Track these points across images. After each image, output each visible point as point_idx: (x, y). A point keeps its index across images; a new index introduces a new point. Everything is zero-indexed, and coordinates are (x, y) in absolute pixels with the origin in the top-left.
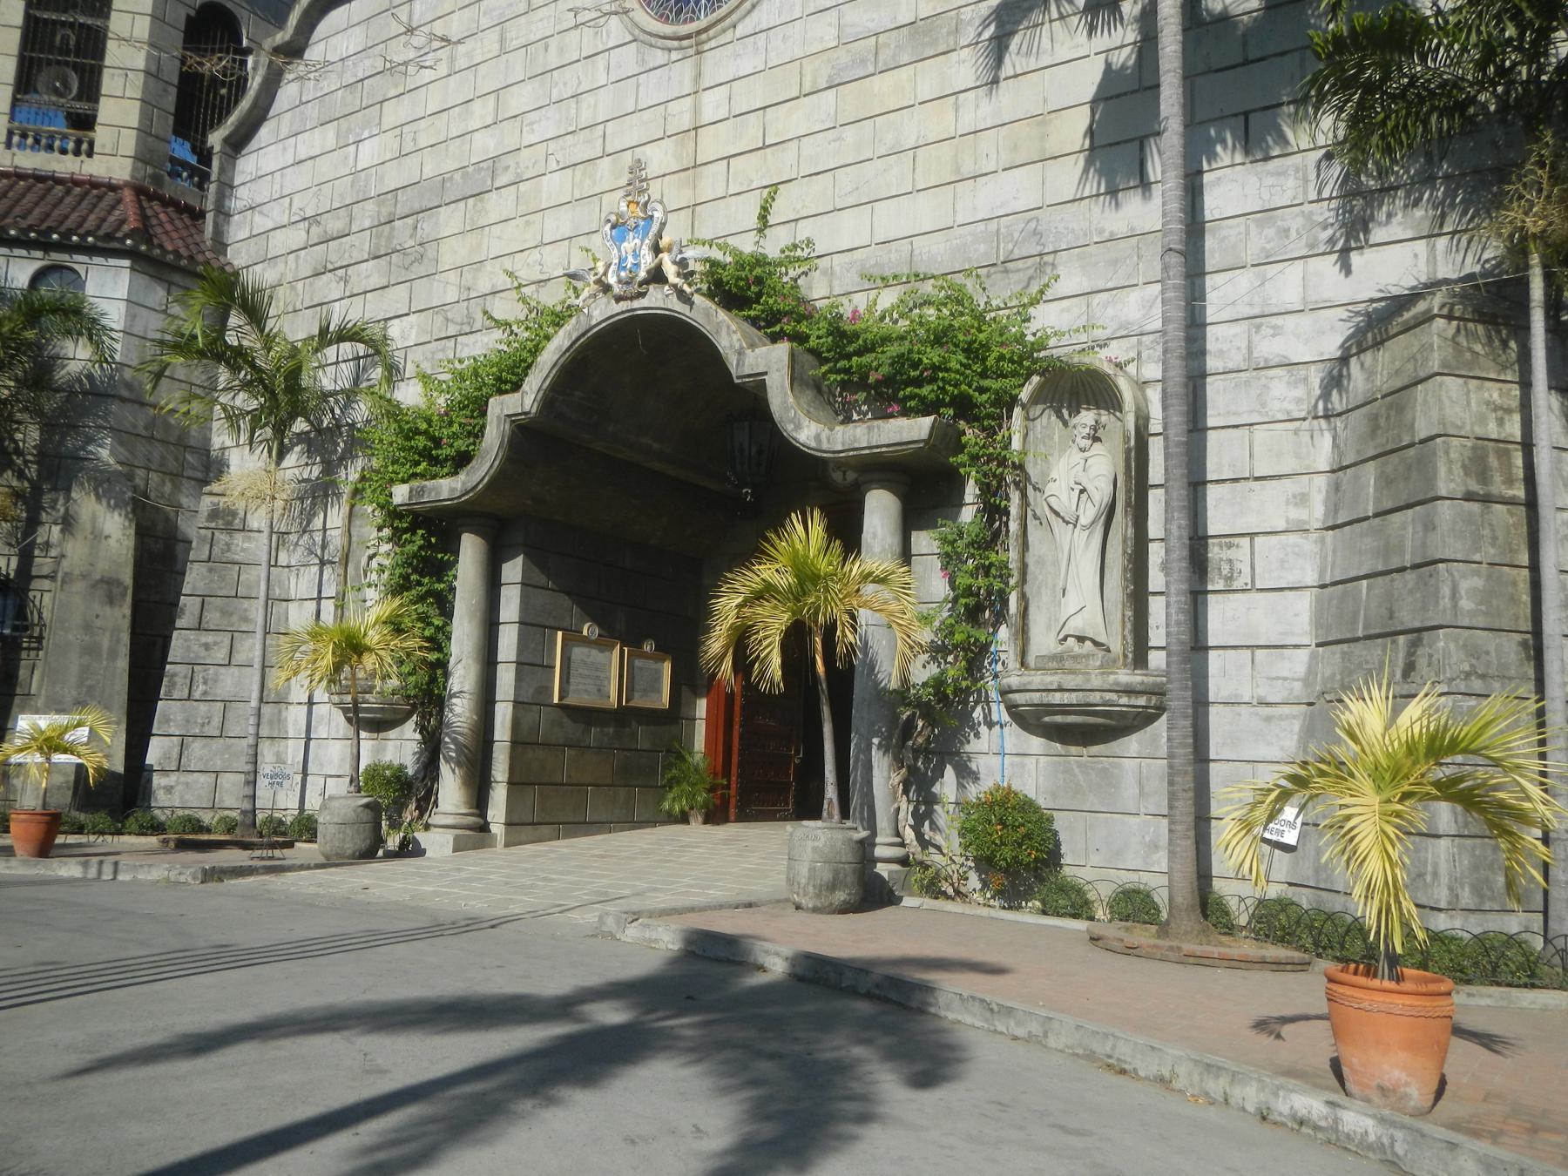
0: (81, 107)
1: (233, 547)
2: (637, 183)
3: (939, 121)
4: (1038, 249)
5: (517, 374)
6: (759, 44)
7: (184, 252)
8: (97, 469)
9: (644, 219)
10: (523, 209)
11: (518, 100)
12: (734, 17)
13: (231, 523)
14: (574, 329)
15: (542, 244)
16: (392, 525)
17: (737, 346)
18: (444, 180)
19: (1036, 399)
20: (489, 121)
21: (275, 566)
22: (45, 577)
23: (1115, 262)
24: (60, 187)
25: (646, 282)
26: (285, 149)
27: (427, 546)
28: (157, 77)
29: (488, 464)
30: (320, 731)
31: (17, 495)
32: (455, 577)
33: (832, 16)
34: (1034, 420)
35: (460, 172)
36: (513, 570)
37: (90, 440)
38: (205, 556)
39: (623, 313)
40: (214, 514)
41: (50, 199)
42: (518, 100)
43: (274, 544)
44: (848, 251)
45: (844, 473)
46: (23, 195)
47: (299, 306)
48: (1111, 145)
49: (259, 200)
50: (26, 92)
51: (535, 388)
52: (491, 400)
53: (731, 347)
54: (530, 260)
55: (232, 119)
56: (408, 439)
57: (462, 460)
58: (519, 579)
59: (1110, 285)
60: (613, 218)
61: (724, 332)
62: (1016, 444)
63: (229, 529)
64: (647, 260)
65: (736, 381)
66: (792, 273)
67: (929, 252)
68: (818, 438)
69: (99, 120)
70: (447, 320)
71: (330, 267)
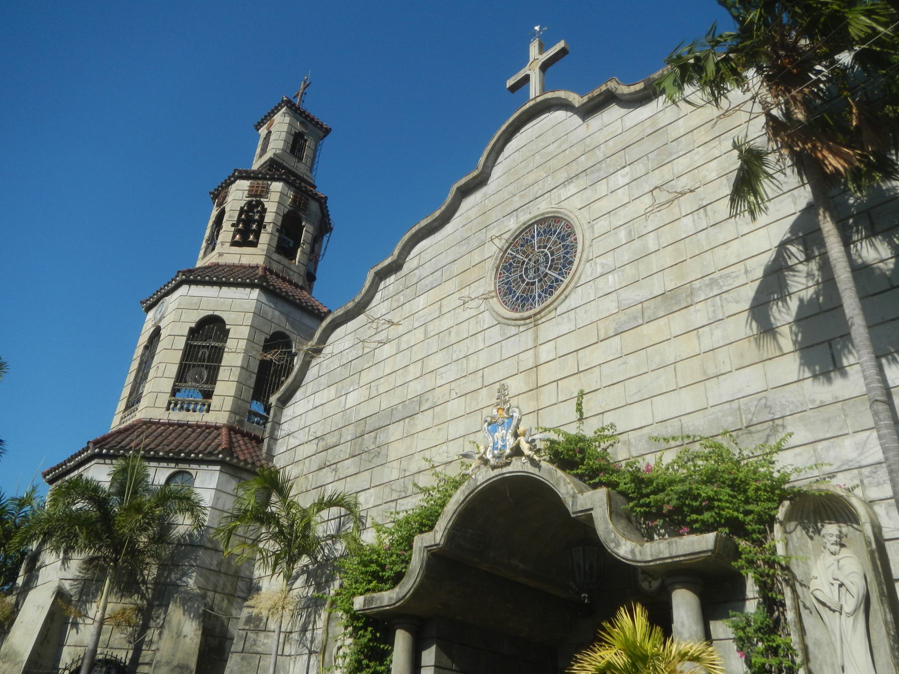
0: (206, 387)
1: (258, 642)
2: (503, 398)
3: (689, 346)
4: (770, 417)
5: (432, 521)
6: (571, 316)
7: (250, 461)
8: (186, 592)
9: (507, 418)
10: (436, 422)
11: (434, 362)
12: (555, 304)
13: (258, 626)
14: (467, 489)
15: (448, 441)
16: (352, 625)
17: (571, 492)
18: (392, 409)
19: (789, 517)
20: (418, 375)
21: (282, 655)
22: (146, 664)
23: (828, 420)
24: (190, 429)
25: (510, 456)
26: (308, 401)
27: (373, 639)
28: (247, 370)
29: (413, 581)
31: (139, 610)
32: (391, 661)
33: (613, 296)
34: (790, 533)
35: (401, 405)
36: (429, 656)
37: (185, 574)
38: (240, 649)
39: (496, 476)
40: (249, 620)
41: (184, 435)
42: (434, 362)
43: (281, 640)
44: (639, 429)
45: (650, 582)
46: (171, 434)
47: (309, 488)
48: (808, 347)
49: (293, 430)
50: (180, 382)
51: (443, 528)
52: (416, 537)
53: (568, 493)
54: (441, 451)
55: (283, 388)
56: (365, 566)
57: (398, 578)
58: (433, 663)
59: (828, 436)
60: (489, 419)
61: (562, 484)
62: (780, 551)
63: (257, 630)
64: (511, 442)
65: (573, 516)
66: (603, 446)
67: (693, 425)
68: (632, 552)
69: (214, 393)
70: (392, 490)
71: (328, 464)
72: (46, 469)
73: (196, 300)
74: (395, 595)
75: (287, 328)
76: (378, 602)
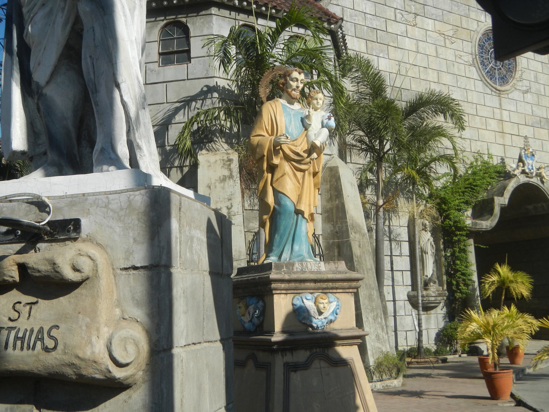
30: (401, 312)
74: (489, 225)
76: (480, 226)
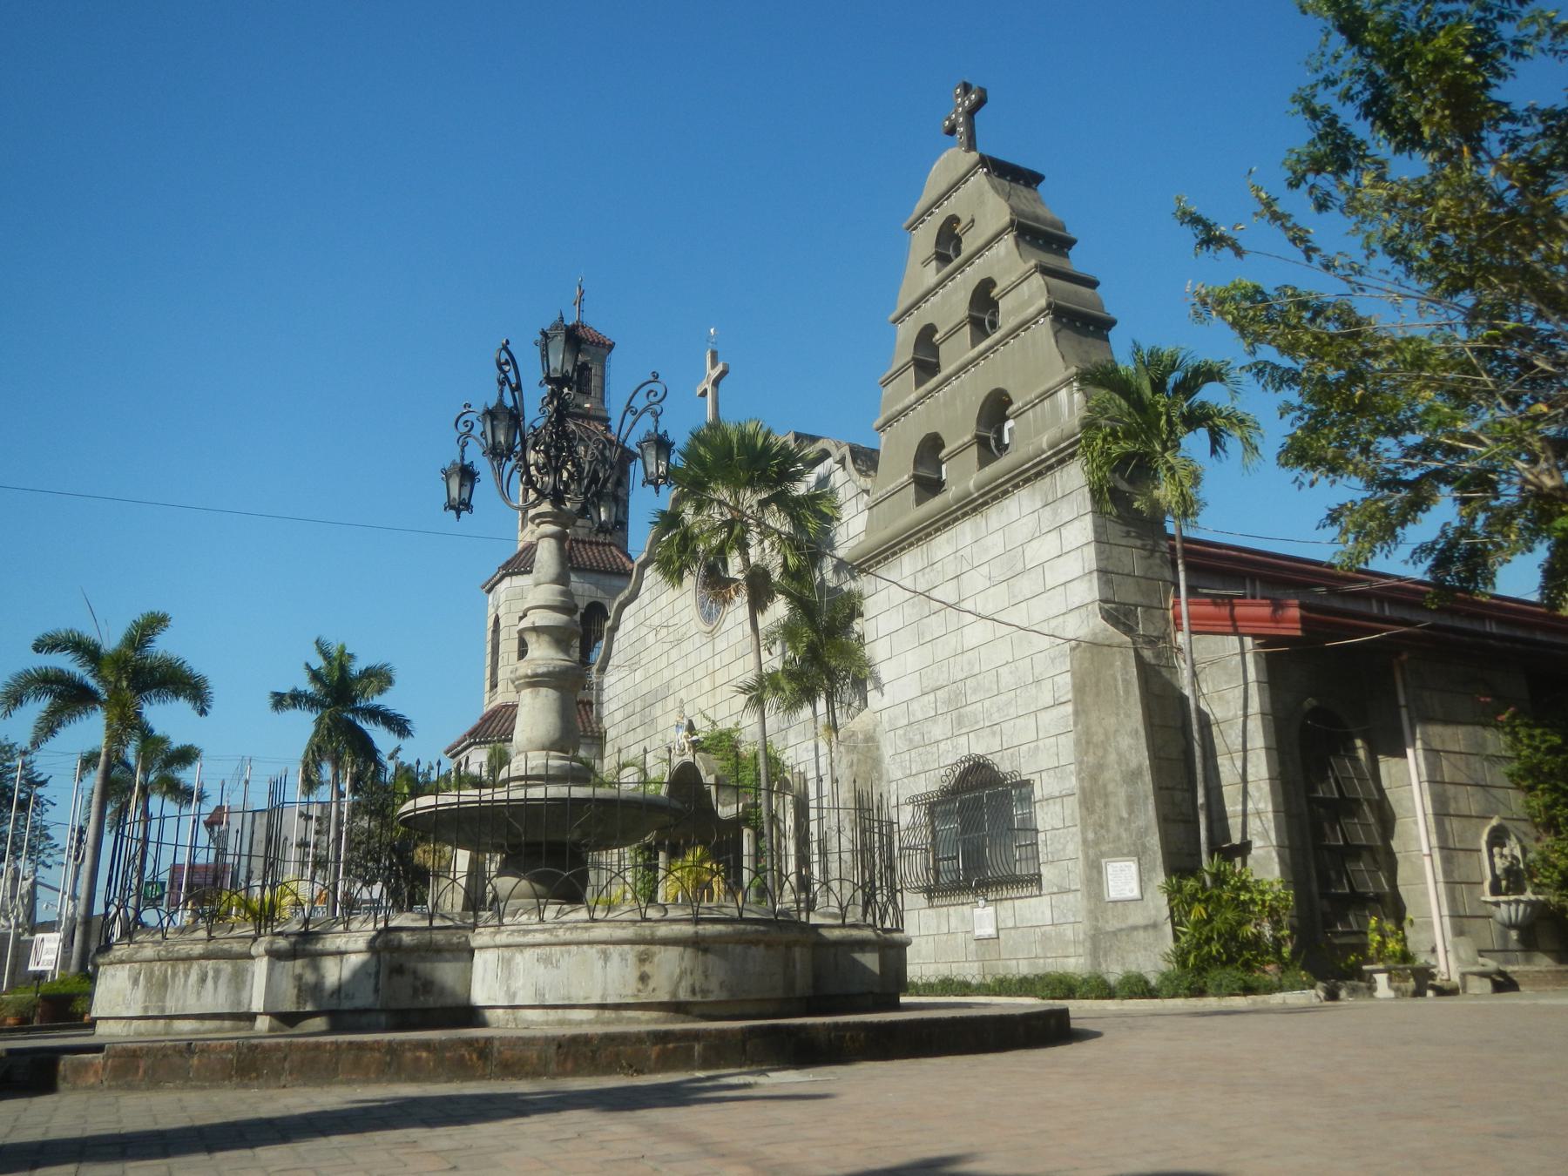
72: (446, 747)
73: (518, 590)
75: (599, 595)
